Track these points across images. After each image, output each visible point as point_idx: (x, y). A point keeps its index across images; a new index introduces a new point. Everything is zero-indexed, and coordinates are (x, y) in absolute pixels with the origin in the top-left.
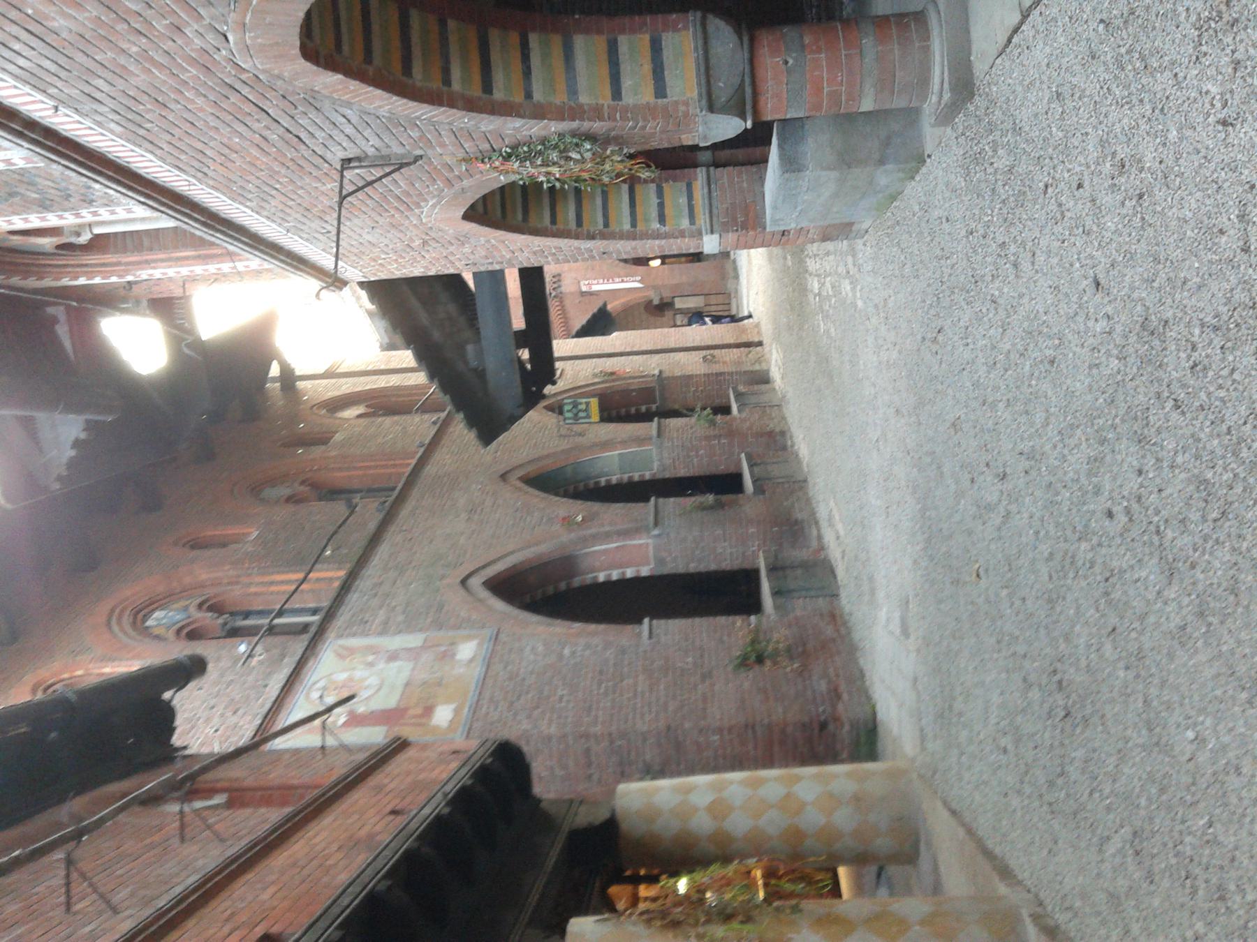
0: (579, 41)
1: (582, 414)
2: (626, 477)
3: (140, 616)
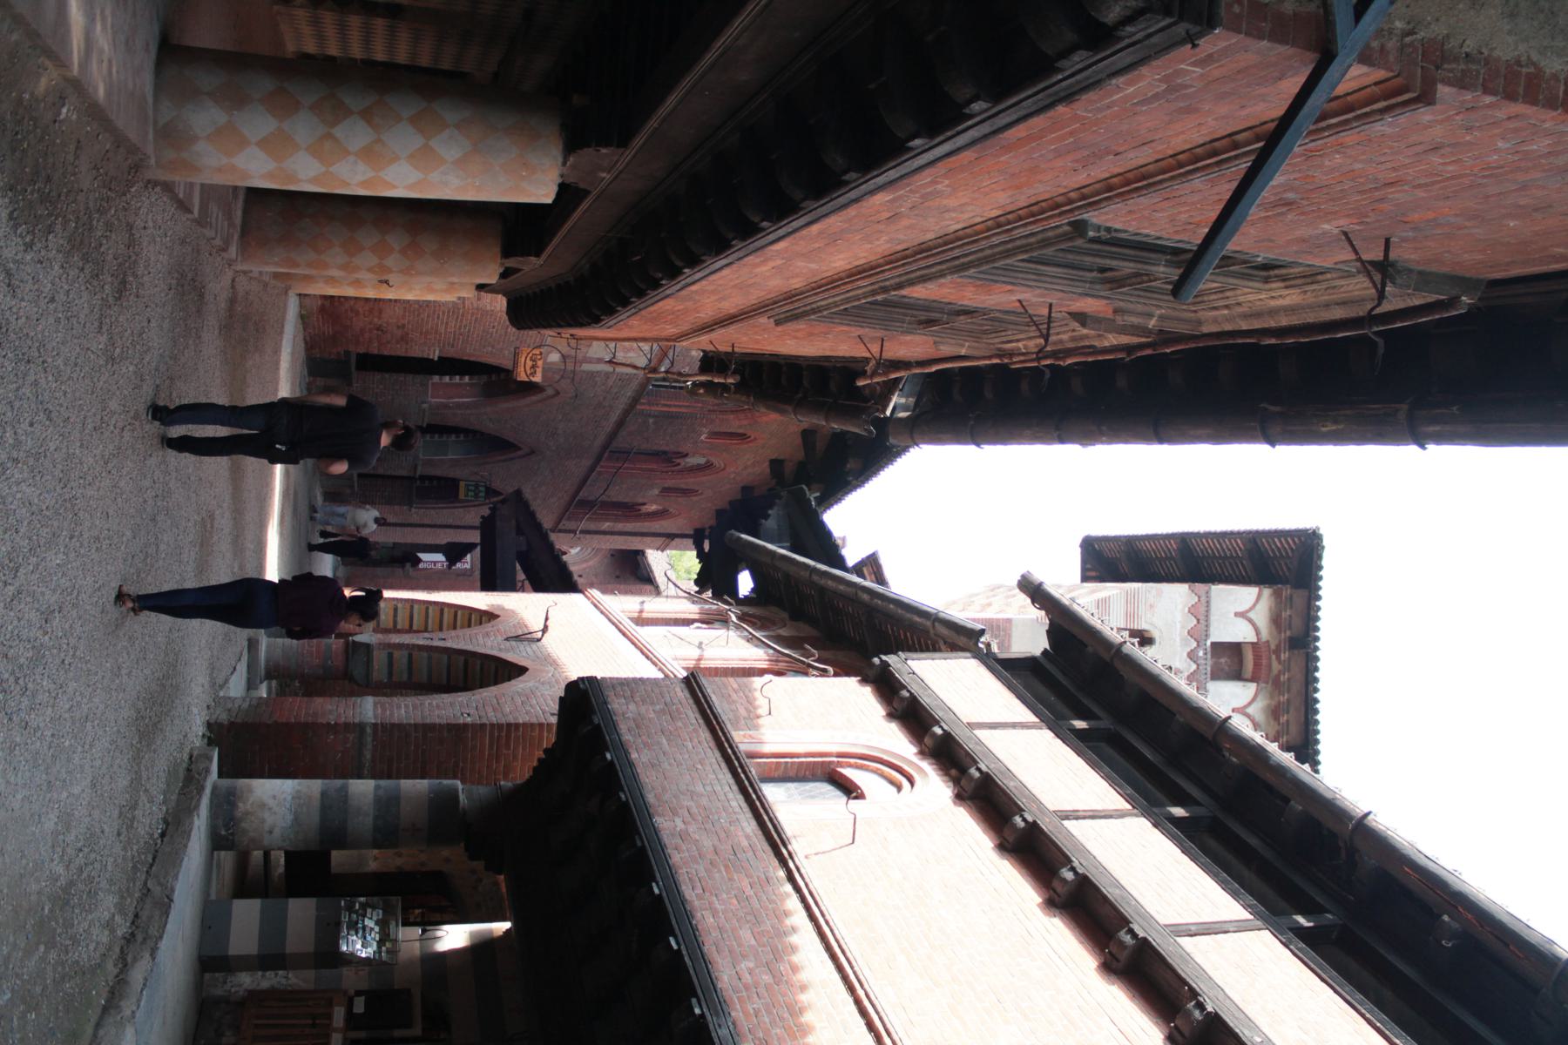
2: (445, 438)
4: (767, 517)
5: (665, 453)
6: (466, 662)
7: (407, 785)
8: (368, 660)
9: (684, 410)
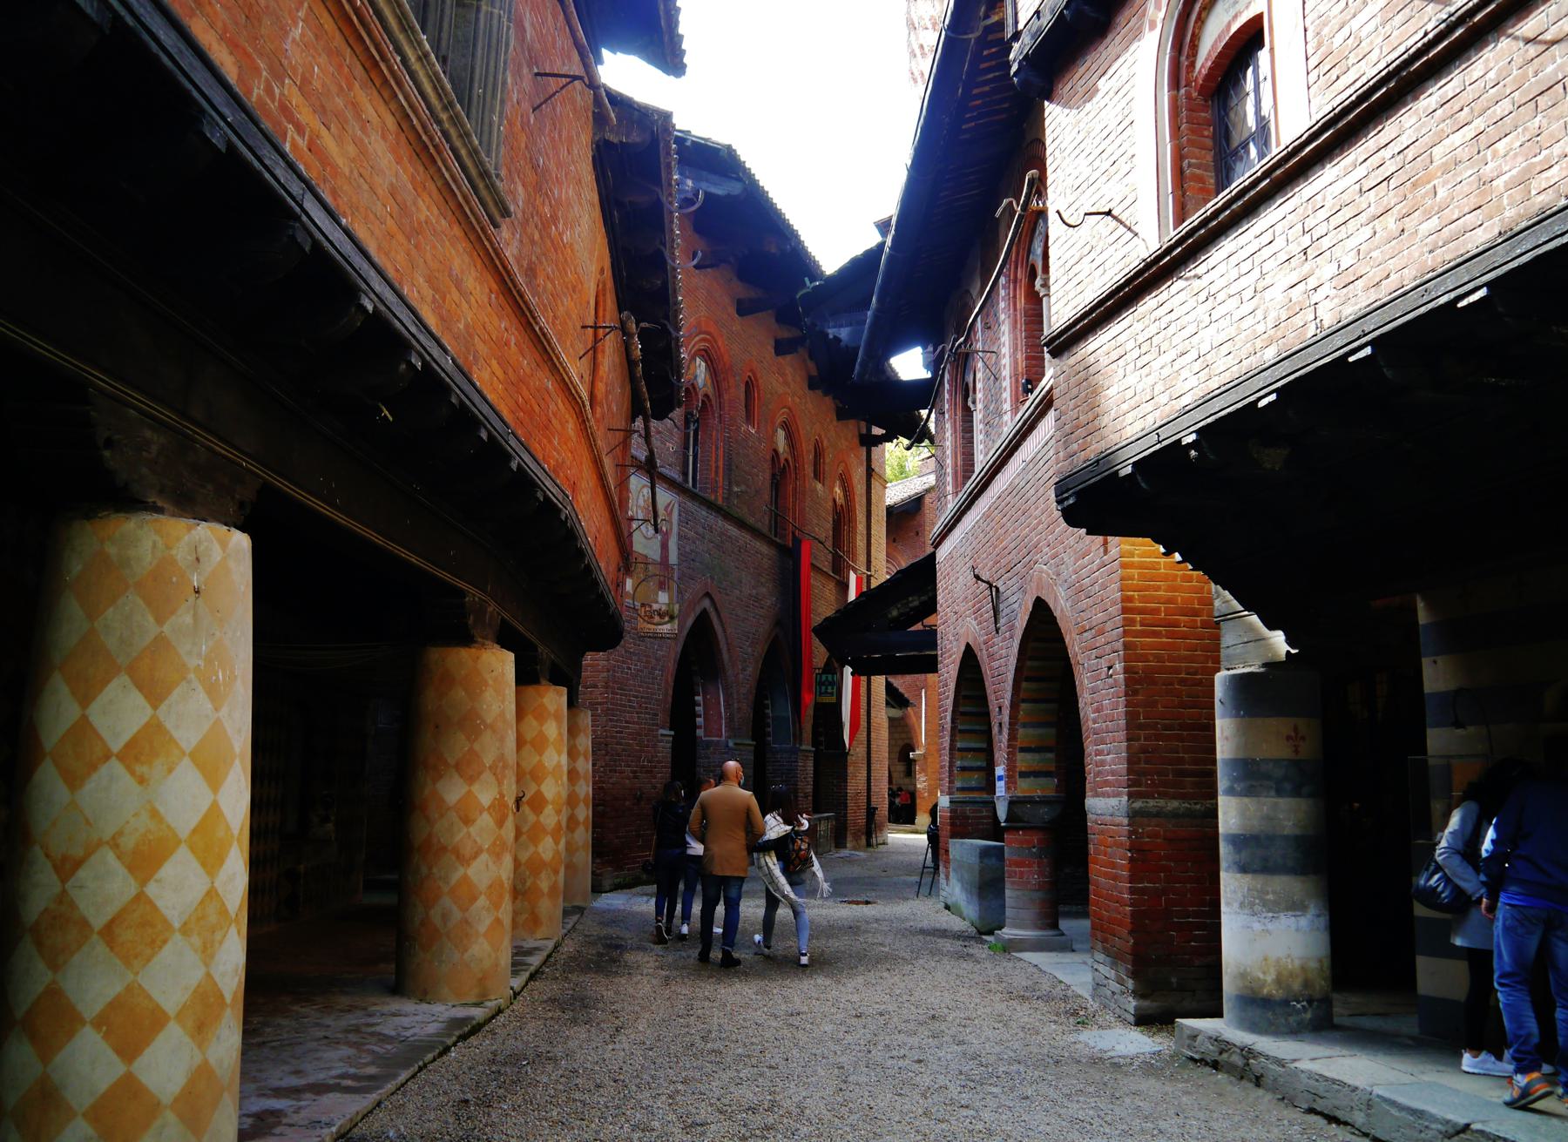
0: (1053, 731)
1: (823, 688)
2: (770, 721)
3: (703, 353)
4: (837, 340)
5: (773, 475)
6: (1027, 679)
7: (1224, 748)
8: (1029, 802)
9: (720, 452)
